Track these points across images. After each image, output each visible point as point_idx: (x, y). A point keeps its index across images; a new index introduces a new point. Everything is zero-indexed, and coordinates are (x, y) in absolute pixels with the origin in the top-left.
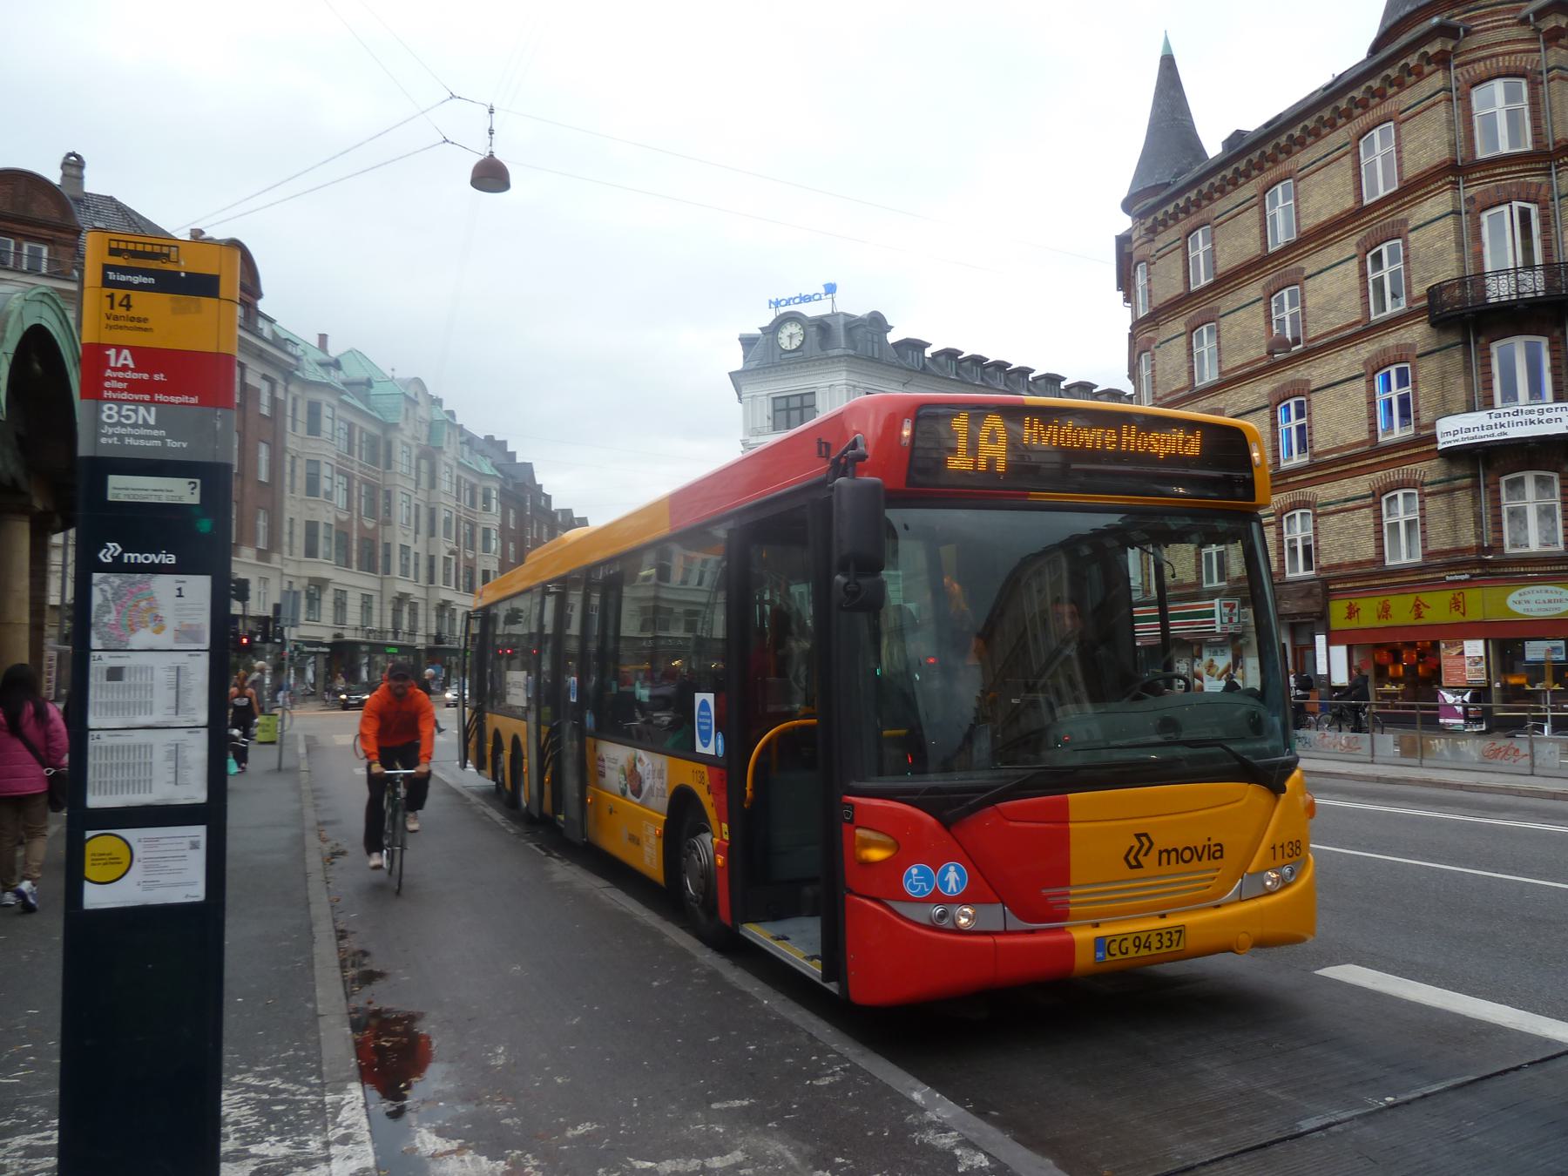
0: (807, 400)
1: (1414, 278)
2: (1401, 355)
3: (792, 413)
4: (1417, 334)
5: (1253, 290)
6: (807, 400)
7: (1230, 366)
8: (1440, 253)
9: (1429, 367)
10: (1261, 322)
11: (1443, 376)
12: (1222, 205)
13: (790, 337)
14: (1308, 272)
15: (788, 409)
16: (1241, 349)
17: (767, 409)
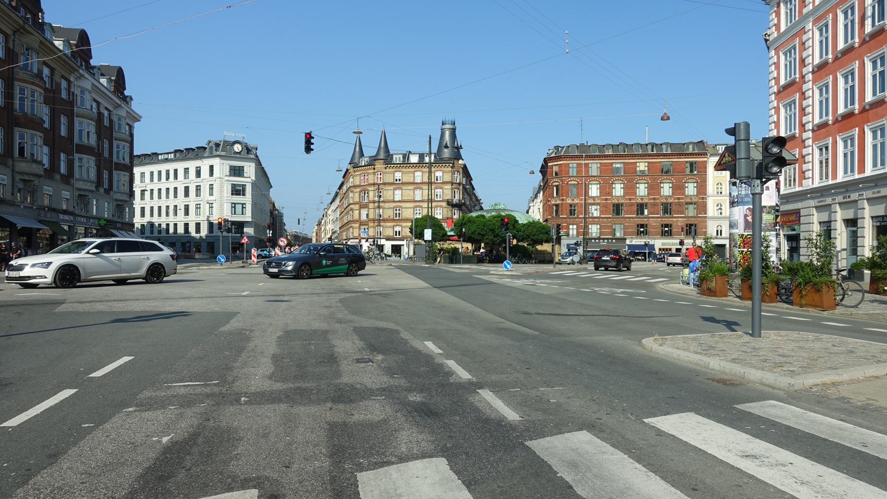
0: (241, 168)
1: (444, 196)
2: (441, 206)
3: (236, 171)
4: (444, 204)
5: (411, 187)
6: (241, 168)
7: (405, 199)
8: (448, 194)
9: (445, 209)
10: (413, 194)
11: (447, 211)
12: (404, 170)
13: (237, 148)
14: (424, 188)
15: (235, 170)
16: (407, 197)
17: (228, 169)
